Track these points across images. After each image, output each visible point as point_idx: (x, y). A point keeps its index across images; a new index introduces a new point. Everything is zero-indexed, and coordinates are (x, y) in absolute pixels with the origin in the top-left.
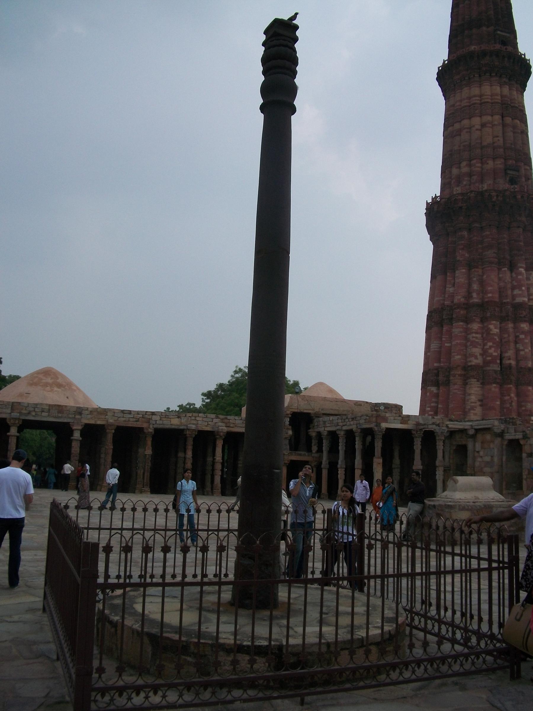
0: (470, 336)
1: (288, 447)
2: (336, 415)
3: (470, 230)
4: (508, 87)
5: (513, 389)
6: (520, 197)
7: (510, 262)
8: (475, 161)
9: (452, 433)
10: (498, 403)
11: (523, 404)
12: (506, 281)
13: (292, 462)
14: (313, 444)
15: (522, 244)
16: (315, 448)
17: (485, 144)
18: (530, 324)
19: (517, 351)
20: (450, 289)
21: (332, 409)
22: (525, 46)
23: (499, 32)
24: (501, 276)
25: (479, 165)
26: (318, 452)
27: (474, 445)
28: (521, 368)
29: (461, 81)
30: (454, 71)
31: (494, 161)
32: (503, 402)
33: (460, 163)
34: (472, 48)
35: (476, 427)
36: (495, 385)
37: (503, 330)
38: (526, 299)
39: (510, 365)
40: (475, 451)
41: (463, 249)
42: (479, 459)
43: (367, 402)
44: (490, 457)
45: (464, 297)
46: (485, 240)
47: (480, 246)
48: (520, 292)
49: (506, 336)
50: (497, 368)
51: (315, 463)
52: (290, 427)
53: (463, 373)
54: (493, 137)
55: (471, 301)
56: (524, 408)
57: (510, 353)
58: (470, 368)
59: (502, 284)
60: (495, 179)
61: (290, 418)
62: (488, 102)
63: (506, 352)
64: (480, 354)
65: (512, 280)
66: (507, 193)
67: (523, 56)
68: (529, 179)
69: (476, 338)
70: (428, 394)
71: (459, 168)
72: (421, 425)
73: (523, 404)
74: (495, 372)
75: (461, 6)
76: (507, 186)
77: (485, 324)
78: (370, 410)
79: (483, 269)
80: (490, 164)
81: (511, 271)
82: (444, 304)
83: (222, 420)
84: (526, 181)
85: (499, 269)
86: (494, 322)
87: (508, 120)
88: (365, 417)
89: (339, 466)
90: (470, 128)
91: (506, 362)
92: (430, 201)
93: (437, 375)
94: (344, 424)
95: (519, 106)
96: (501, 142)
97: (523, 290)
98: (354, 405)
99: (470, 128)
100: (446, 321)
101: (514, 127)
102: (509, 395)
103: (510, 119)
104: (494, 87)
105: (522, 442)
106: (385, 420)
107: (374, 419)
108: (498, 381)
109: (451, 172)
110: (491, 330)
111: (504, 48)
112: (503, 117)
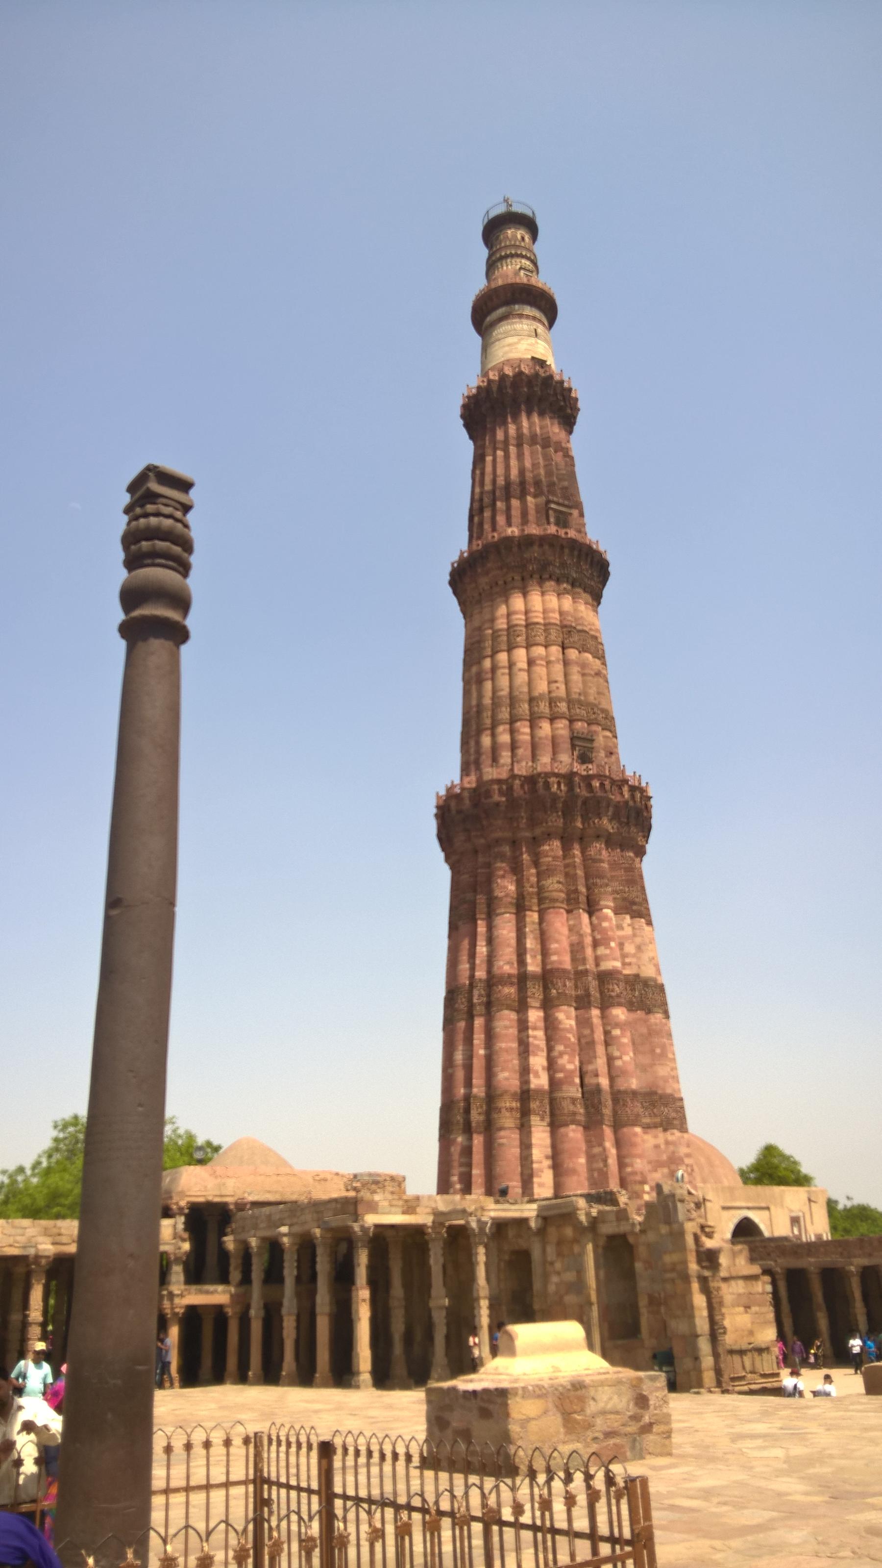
0: (524, 1034)
1: (182, 1278)
3: (515, 844)
4: (570, 598)
5: (608, 1132)
6: (598, 785)
7: (588, 897)
8: (518, 724)
9: (501, 1226)
10: (582, 1160)
11: (627, 1160)
12: (582, 932)
13: (192, 1310)
14: (232, 1268)
15: (605, 865)
16: (235, 1275)
17: (536, 694)
18: (630, 1010)
19: (610, 1060)
20: (482, 949)
21: (269, 1192)
22: (598, 529)
23: (553, 506)
24: (571, 922)
25: (528, 730)
27: (544, 1251)
28: (619, 1091)
29: (491, 587)
30: (479, 570)
31: (551, 724)
32: (591, 1158)
33: (493, 728)
34: (509, 531)
35: (545, 1214)
36: (573, 1127)
37: (583, 1023)
38: (618, 964)
39: (598, 1089)
40: (544, 1262)
41: (503, 877)
42: (555, 1279)
43: (337, 1174)
44: (575, 1273)
45: (508, 963)
46: (542, 860)
47: (533, 871)
48: (608, 952)
49: (587, 1032)
50: (575, 1092)
52: (186, 1235)
53: (515, 1104)
54: (549, 683)
55: (522, 970)
56: (629, 1169)
59: (575, 938)
60: (554, 753)
62: (537, 623)
63: (590, 1062)
64: (543, 1068)
65: (593, 931)
67: (594, 547)
68: (611, 753)
69: (535, 1037)
70: (453, 1149)
71: (493, 735)
72: (442, 1214)
73: (627, 1160)
74: (573, 1100)
75: (489, 459)
76: (577, 767)
78: (342, 1187)
80: (545, 729)
81: (590, 916)
82: (472, 977)
83: (46, 1232)
84: (606, 756)
85: (569, 912)
86: (565, 1008)
87: (573, 654)
88: (333, 1205)
89: (284, 1311)
91: (588, 1080)
92: (443, 792)
93: (467, 1111)
94: (295, 1220)
95: (591, 629)
96: (562, 692)
97: (611, 948)
98: (311, 1181)
100: (478, 1008)
101: (584, 665)
103: (577, 652)
104: (547, 597)
105: (631, 1240)
106: (373, 1208)
107: (351, 1208)
108: (578, 1118)
109: (478, 743)
110: (560, 1022)
112: (563, 648)
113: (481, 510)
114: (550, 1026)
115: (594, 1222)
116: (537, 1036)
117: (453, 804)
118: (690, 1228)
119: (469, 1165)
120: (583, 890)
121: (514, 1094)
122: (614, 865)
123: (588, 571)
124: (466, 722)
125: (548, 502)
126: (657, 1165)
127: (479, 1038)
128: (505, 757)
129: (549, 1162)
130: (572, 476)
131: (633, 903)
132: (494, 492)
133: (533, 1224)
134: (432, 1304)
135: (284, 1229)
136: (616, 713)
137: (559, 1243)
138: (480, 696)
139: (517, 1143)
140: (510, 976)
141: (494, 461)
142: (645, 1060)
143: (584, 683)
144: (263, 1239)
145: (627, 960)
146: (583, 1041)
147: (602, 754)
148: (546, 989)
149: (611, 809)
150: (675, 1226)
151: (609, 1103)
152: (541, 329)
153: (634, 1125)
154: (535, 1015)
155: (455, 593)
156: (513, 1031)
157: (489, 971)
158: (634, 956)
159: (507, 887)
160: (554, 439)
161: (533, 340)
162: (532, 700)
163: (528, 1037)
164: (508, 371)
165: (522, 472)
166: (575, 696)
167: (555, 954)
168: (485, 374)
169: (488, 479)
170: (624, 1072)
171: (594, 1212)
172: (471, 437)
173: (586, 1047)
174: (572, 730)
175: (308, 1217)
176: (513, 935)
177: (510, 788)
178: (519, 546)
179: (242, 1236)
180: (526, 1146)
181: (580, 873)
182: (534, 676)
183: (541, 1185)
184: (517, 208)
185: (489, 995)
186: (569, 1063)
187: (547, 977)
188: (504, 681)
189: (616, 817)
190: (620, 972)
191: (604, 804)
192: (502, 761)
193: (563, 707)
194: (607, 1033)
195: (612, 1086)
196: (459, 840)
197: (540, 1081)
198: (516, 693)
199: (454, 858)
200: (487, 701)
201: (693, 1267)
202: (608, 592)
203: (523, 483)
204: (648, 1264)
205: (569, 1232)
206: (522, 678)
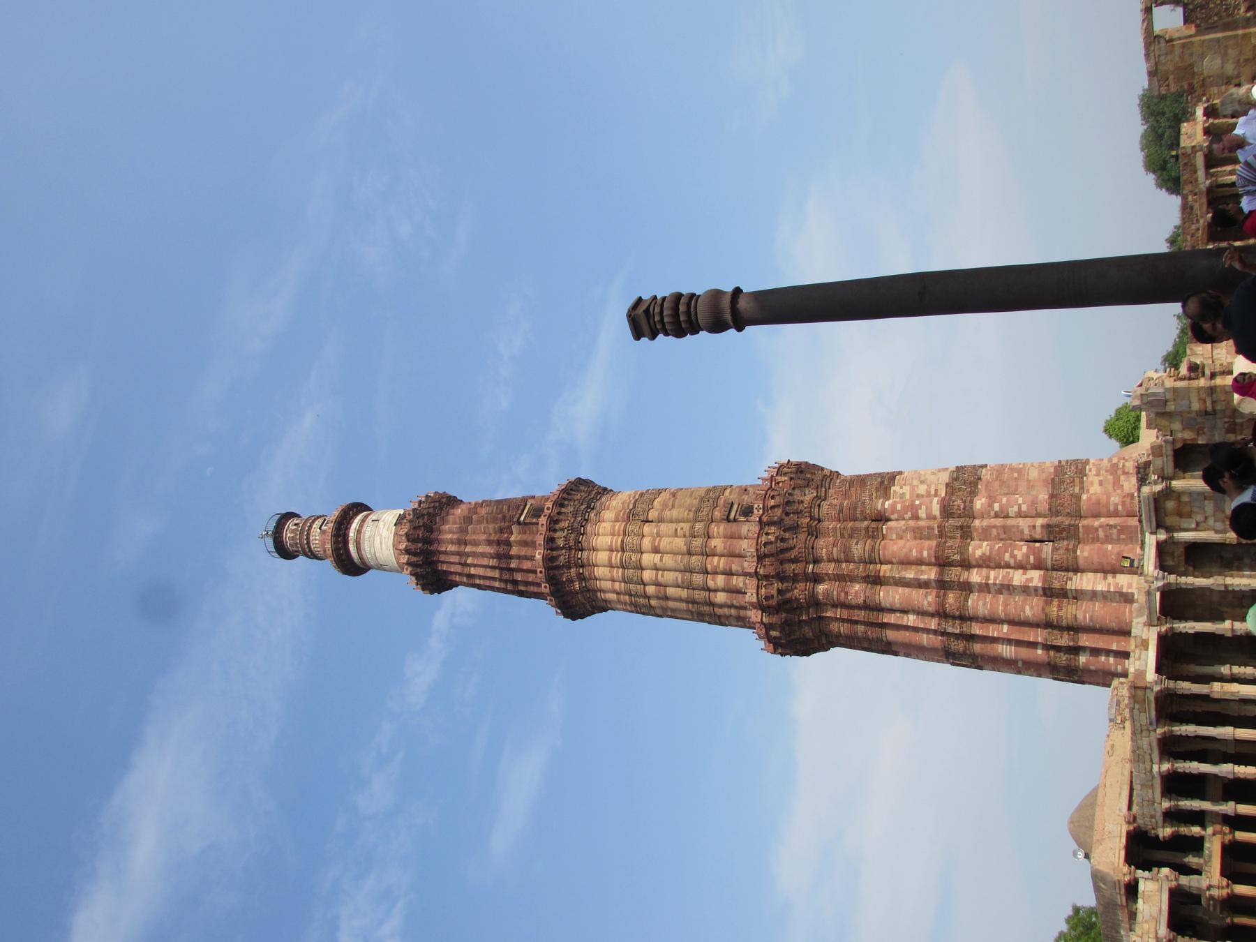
0: (992, 590)
2: (1131, 790)
3: (817, 579)
8: (709, 567)
10: (1110, 547)
11: (1112, 508)
19: (1020, 515)
20: (911, 619)
22: (548, 485)
25: (716, 559)
26: (1204, 827)
28: (1050, 509)
32: (1108, 540)
33: (709, 590)
34: (538, 557)
35: (1154, 524)
37: (985, 535)
38: (936, 500)
41: (846, 593)
49: (994, 532)
51: (1226, 829)
52: (1155, 870)
53: (1055, 602)
56: (1120, 508)
57: (1024, 524)
58: (1048, 592)
59: (909, 535)
60: (740, 538)
61: (1137, 868)
63: (1022, 532)
66: (765, 519)
69: (995, 578)
71: (716, 591)
73: (1112, 508)
74: (1054, 550)
75: (473, 571)
77: (974, 563)
79: (881, 564)
80: (717, 543)
81: (888, 520)
82: (935, 632)
87: (653, 514)
90: (657, 569)
91: (1038, 534)
92: (762, 644)
93: (1058, 649)
94: (1147, 757)
96: (686, 526)
97: (921, 504)
99: (657, 569)
101: (665, 505)
102: (1097, 530)
105: (1179, 445)
106: (1141, 674)
107: (1140, 692)
108: (1071, 547)
109: (721, 606)
111: (547, 512)
113: (515, 582)
114: (986, 563)
115: (1163, 478)
116: (996, 576)
117: (774, 633)
118: (1169, 383)
119: (1108, 652)
120: (866, 523)
121: (1046, 603)
122: (846, 495)
123: (582, 496)
124: (700, 617)
125: (519, 523)
126: (1116, 483)
127: (993, 631)
128: (738, 582)
129: (1110, 577)
130: (499, 502)
131: (882, 483)
132: (501, 569)
133: (1162, 536)
134: (1229, 635)
135: (1156, 768)
136: (710, 485)
137: (1180, 515)
138: (680, 600)
139: (1090, 604)
140: (938, 596)
141: (475, 566)
142: (1023, 486)
143: (680, 506)
144: (1163, 795)
145: (933, 492)
146: (1002, 536)
147: (746, 497)
148: (951, 564)
149: (797, 492)
150: (1169, 396)
151: (1059, 518)
152: (373, 517)
153: (1077, 497)
154: (975, 577)
155: (583, 617)
156: (989, 598)
157: (932, 615)
158: (929, 486)
159: (857, 591)
160: (466, 513)
161: (381, 524)
162: (690, 553)
163: (995, 584)
164: (403, 546)
165: (489, 543)
166: (691, 515)
167: (921, 553)
168: (401, 568)
169: (490, 573)
170: (1033, 503)
171: (1154, 477)
172: (450, 588)
173: (1008, 535)
174: (721, 520)
175: (1145, 742)
176: (900, 590)
177: (766, 577)
178: (552, 549)
179: (1160, 818)
180: (1094, 595)
181: (851, 524)
182: (668, 548)
183: (1130, 586)
184: (271, 528)
185: (954, 618)
186: (1021, 551)
187: (942, 563)
188: (670, 577)
189: (801, 487)
190: (943, 499)
191: (791, 498)
192: (741, 585)
193: (699, 526)
194: (996, 516)
195: (1045, 516)
196: (807, 632)
197: (1036, 578)
198: (681, 567)
199: (824, 641)
200: (684, 593)
201: (1202, 382)
202: (601, 483)
203: (499, 543)
204: (1200, 431)
205: (1170, 505)
206: (668, 560)
